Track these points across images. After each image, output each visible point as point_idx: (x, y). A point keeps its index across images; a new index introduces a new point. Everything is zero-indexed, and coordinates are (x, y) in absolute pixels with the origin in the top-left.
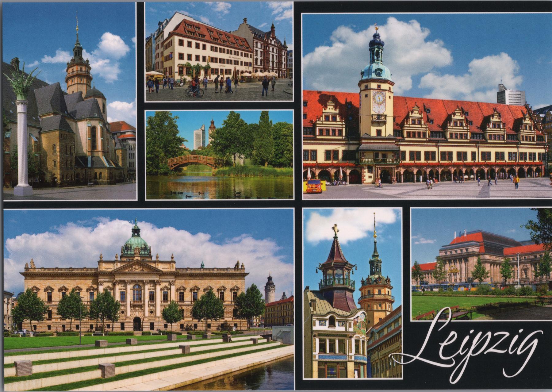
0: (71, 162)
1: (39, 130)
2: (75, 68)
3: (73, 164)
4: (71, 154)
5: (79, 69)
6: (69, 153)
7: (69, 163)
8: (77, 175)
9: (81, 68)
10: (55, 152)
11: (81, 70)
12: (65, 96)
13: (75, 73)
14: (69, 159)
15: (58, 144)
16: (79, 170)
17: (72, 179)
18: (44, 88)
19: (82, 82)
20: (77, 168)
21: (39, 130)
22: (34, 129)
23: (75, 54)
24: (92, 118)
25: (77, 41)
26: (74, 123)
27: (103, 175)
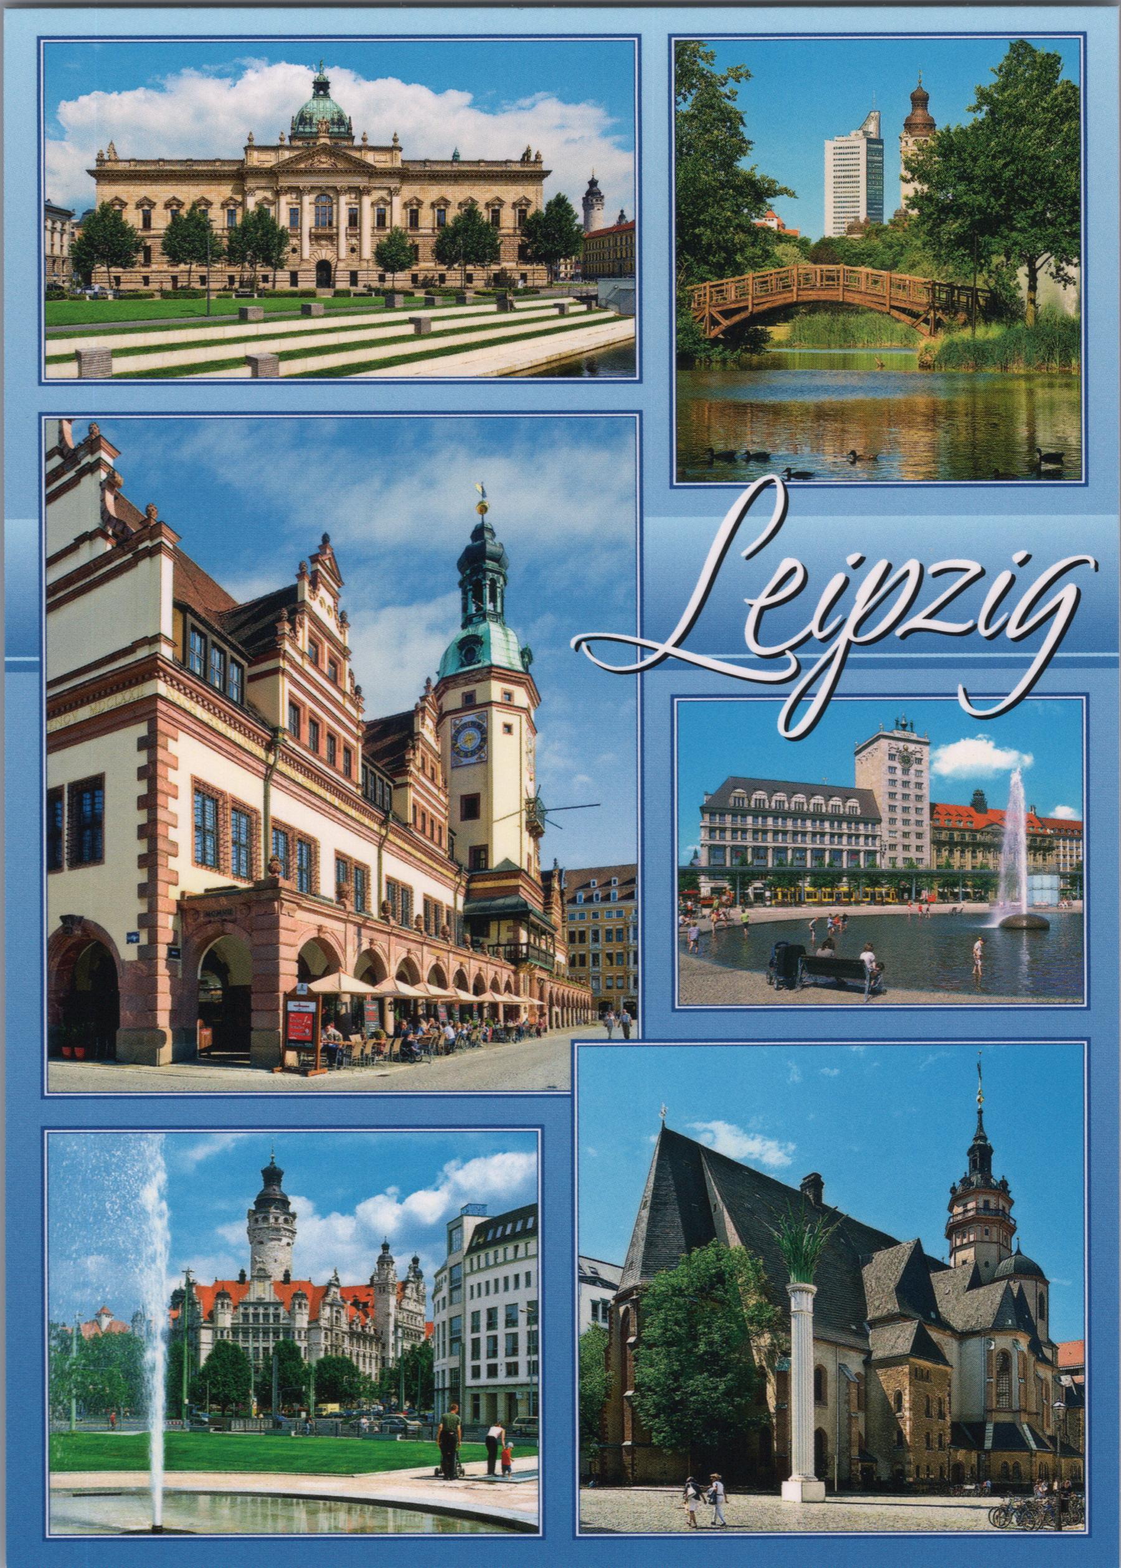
0: (941, 1435)
1: (863, 1357)
3: (947, 1439)
4: (942, 1415)
6: (934, 1412)
7: (934, 1436)
12: (935, 1277)
14: (935, 1428)
15: (907, 1391)
16: (961, 1455)
17: (942, 1475)
22: (852, 1353)
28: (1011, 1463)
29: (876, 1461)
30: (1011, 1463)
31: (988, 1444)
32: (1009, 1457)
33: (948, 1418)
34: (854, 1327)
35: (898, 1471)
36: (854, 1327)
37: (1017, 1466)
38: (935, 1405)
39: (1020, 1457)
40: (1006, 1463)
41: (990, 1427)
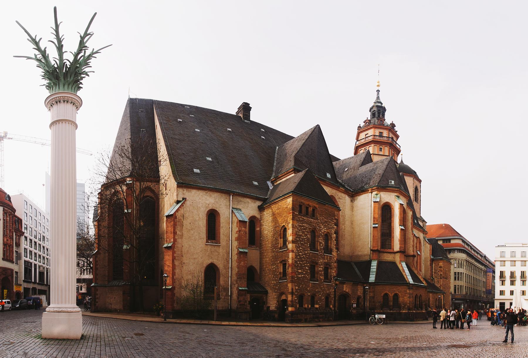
2: (371, 132)
3: (333, 272)
4: (328, 250)
5: (377, 134)
8: (345, 297)
9: (381, 133)
10: (285, 241)
11: (381, 135)
13: (371, 139)
15: (290, 225)
18: (292, 141)
19: (381, 153)
20: (343, 283)
21: (259, 203)
23: (373, 115)
24: (383, 187)
25: (378, 98)
26: (347, 199)
27: (401, 299)
28: (391, 295)
29: (266, 293)
30: (391, 295)
31: (372, 278)
32: (390, 291)
33: (334, 254)
34: (256, 183)
35: (283, 300)
36: (256, 183)
37: (396, 296)
38: (321, 240)
39: (399, 290)
40: (386, 295)
41: (374, 264)
